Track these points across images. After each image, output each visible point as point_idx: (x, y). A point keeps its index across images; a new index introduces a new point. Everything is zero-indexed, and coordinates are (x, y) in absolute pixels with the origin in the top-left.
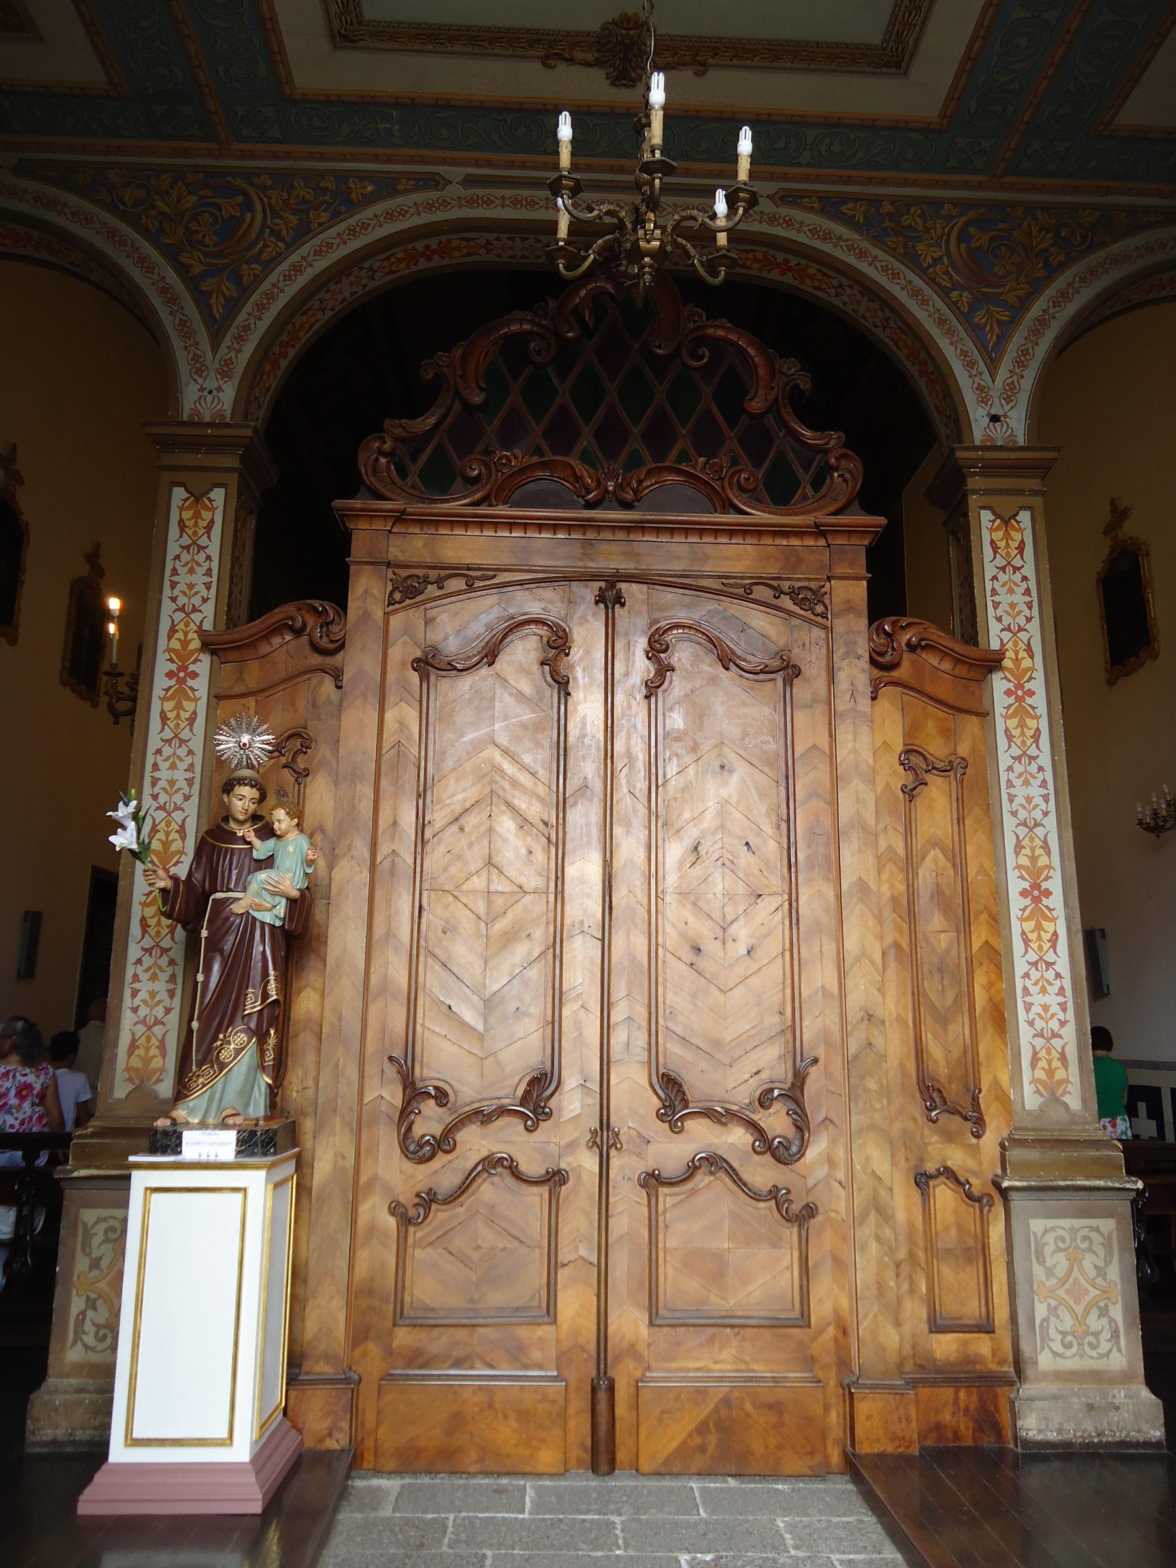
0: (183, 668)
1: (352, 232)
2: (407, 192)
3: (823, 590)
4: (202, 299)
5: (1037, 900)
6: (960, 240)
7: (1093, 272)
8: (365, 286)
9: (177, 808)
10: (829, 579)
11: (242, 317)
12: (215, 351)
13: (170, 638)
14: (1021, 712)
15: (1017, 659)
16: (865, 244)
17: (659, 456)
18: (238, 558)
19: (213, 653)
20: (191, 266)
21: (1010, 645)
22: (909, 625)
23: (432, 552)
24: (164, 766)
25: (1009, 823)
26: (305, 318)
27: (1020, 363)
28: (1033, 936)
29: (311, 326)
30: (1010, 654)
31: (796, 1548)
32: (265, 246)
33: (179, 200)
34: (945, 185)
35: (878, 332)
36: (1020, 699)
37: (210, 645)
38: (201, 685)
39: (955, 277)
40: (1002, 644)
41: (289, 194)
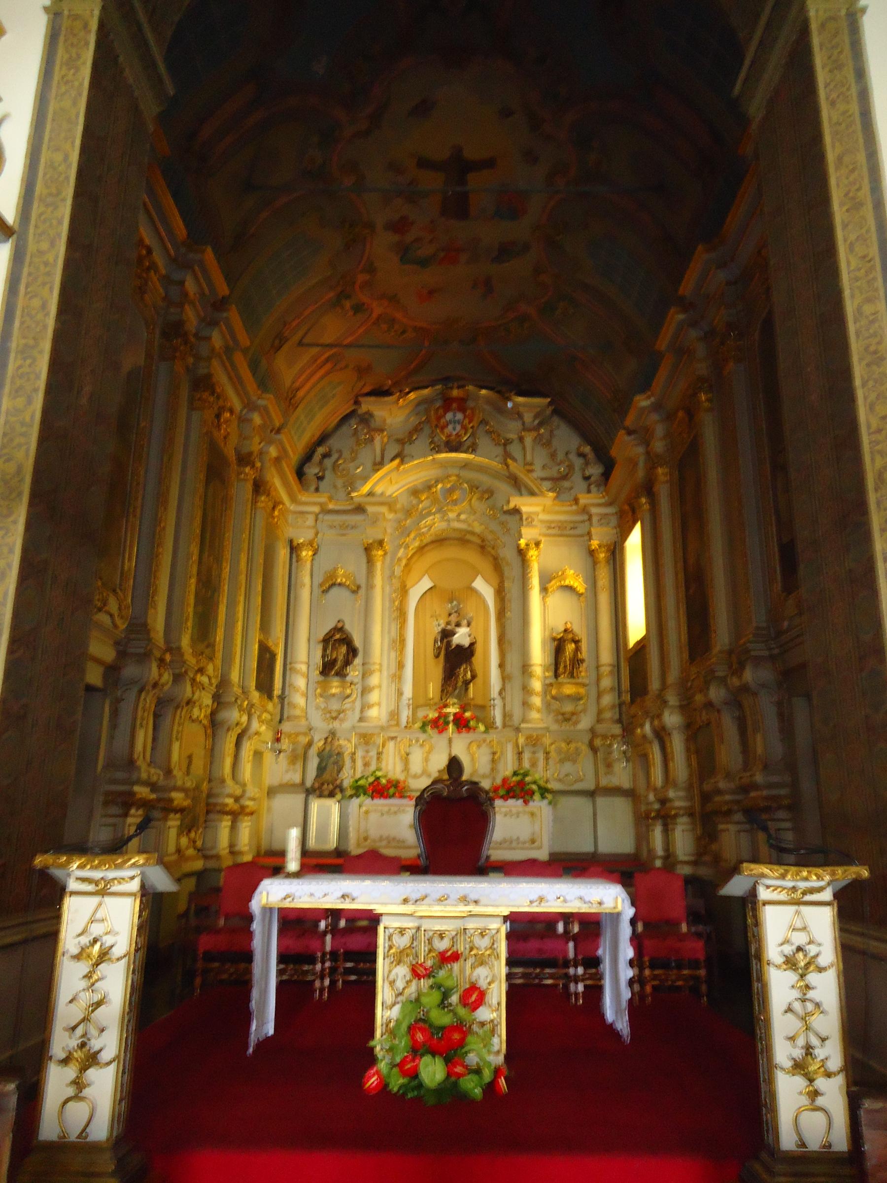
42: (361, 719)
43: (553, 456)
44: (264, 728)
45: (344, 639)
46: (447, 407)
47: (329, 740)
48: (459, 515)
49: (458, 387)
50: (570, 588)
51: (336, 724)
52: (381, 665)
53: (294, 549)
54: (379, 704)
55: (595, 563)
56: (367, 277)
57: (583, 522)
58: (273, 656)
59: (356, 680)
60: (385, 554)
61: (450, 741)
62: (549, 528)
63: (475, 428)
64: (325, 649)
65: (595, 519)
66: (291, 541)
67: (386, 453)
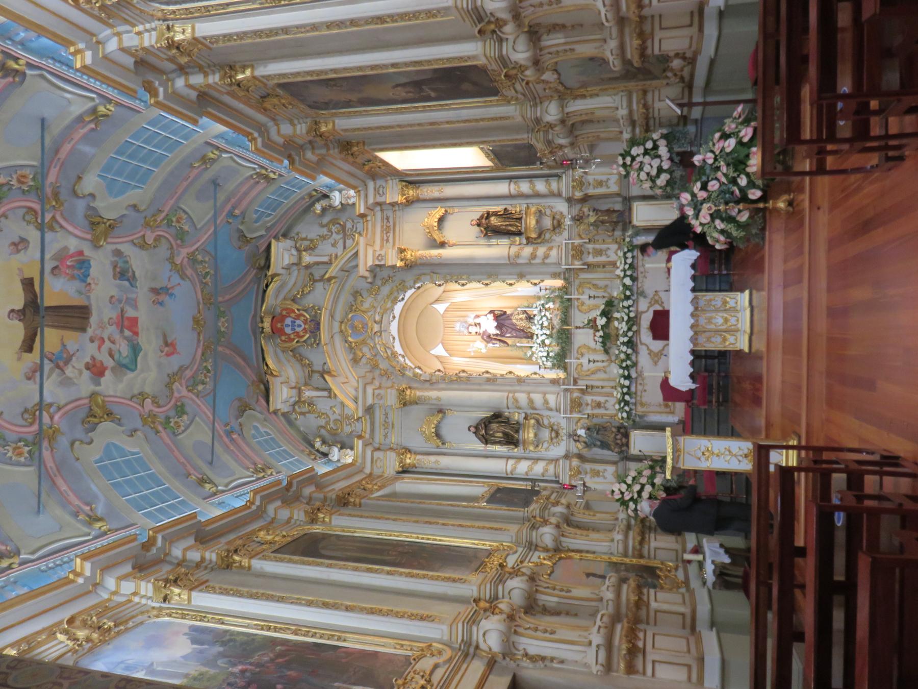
42: (558, 410)
43: (323, 238)
44: (563, 501)
45: (486, 426)
46: (281, 332)
47: (576, 438)
48: (375, 322)
49: (262, 322)
50: (441, 220)
51: (563, 432)
52: (510, 392)
53: (405, 471)
54: (545, 394)
55: (419, 200)
56: (148, 401)
57: (382, 210)
58: (499, 490)
59: (523, 415)
60: (410, 388)
61: (577, 328)
62: (387, 241)
63: (300, 308)
64: (495, 443)
65: (380, 199)
66: (399, 472)
67: (320, 386)
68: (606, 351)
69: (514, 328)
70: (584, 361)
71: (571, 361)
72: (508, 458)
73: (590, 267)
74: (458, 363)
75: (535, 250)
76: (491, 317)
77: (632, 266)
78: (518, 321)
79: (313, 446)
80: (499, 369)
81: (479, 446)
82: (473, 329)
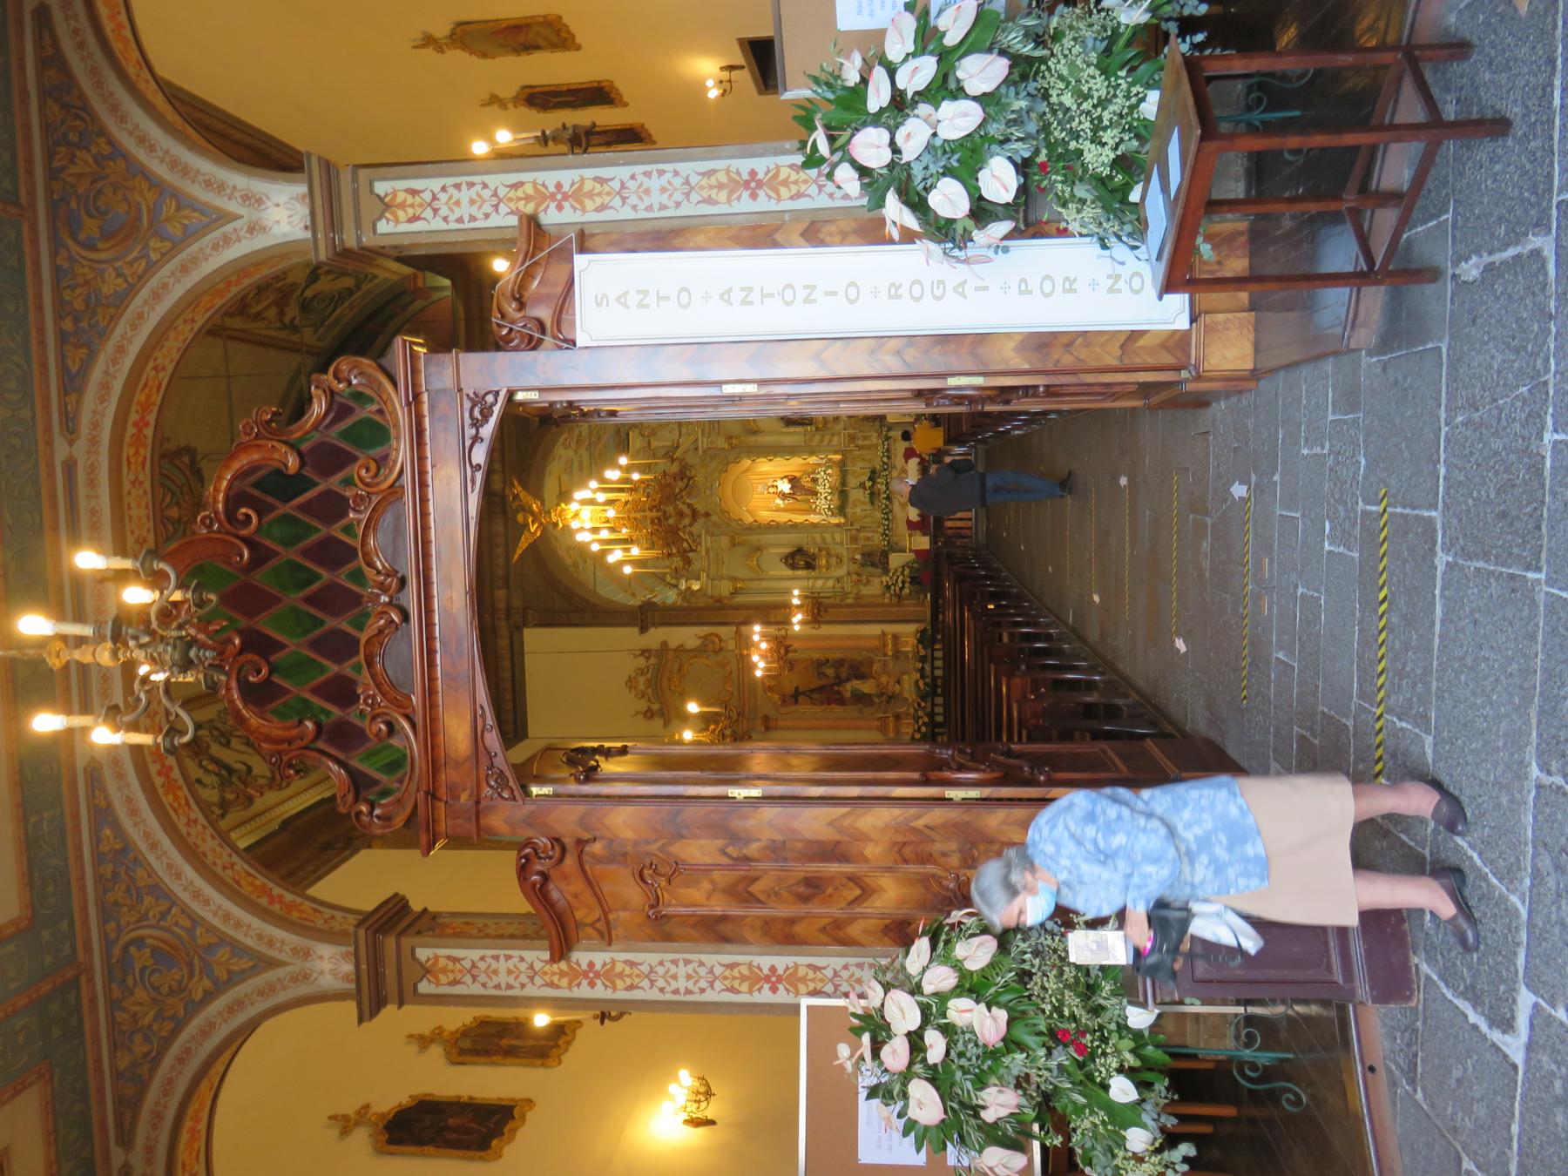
0: (585, 974)
1: (154, 846)
2: (107, 797)
3: (472, 395)
4: (233, 979)
5: (760, 184)
6: (93, 248)
7: (114, 108)
8: (204, 827)
9: (711, 971)
10: (460, 390)
11: (249, 942)
12: (284, 964)
13: (558, 987)
14: (578, 196)
15: (524, 199)
16: (110, 347)
17: (350, 553)
18: (480, 931)
19: (569, 949)
20: (205, 991)
21: (513, 206)
22: (500, 311)
23: (464, 762)
24: (674, 985)
25: (686, 210)
26: (243, 882)
27: (221, 188)
28: (794, 189)
29: (249, 875)
30: (521, 205)
31: (1323, 447)
32: (176, 924)
33: (140, 1004)
34: (37, 265)
35: (197, 326)
36: (566, 197)
37: (561, 950)
38: (600, 958)
39: (134, 254)
40: (512, 213)
41: (124, 905)
51: (845, 559)
68: (872, 502)
69: (803, 488)
70: (858, 510)
71: (849, 511)
72: (809, 578)
73: (860, 448)
74: (765, 516)
75: (823, 436)
76: (786, 480)
77: (888, 450)
78: (806, 482)
79: (664, 580)
80: (799, 518)
81: (790, 572)
82: (771, 490)
